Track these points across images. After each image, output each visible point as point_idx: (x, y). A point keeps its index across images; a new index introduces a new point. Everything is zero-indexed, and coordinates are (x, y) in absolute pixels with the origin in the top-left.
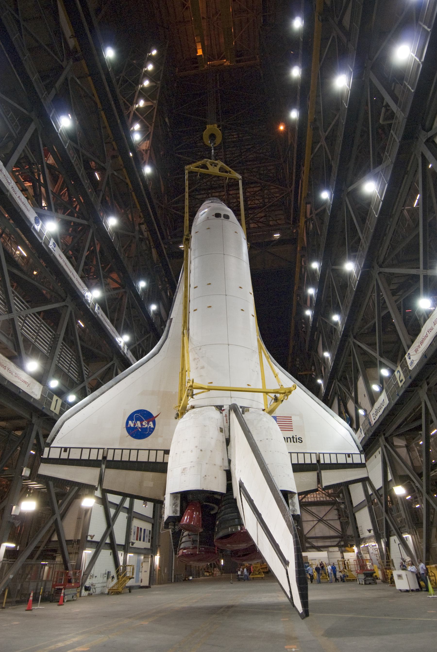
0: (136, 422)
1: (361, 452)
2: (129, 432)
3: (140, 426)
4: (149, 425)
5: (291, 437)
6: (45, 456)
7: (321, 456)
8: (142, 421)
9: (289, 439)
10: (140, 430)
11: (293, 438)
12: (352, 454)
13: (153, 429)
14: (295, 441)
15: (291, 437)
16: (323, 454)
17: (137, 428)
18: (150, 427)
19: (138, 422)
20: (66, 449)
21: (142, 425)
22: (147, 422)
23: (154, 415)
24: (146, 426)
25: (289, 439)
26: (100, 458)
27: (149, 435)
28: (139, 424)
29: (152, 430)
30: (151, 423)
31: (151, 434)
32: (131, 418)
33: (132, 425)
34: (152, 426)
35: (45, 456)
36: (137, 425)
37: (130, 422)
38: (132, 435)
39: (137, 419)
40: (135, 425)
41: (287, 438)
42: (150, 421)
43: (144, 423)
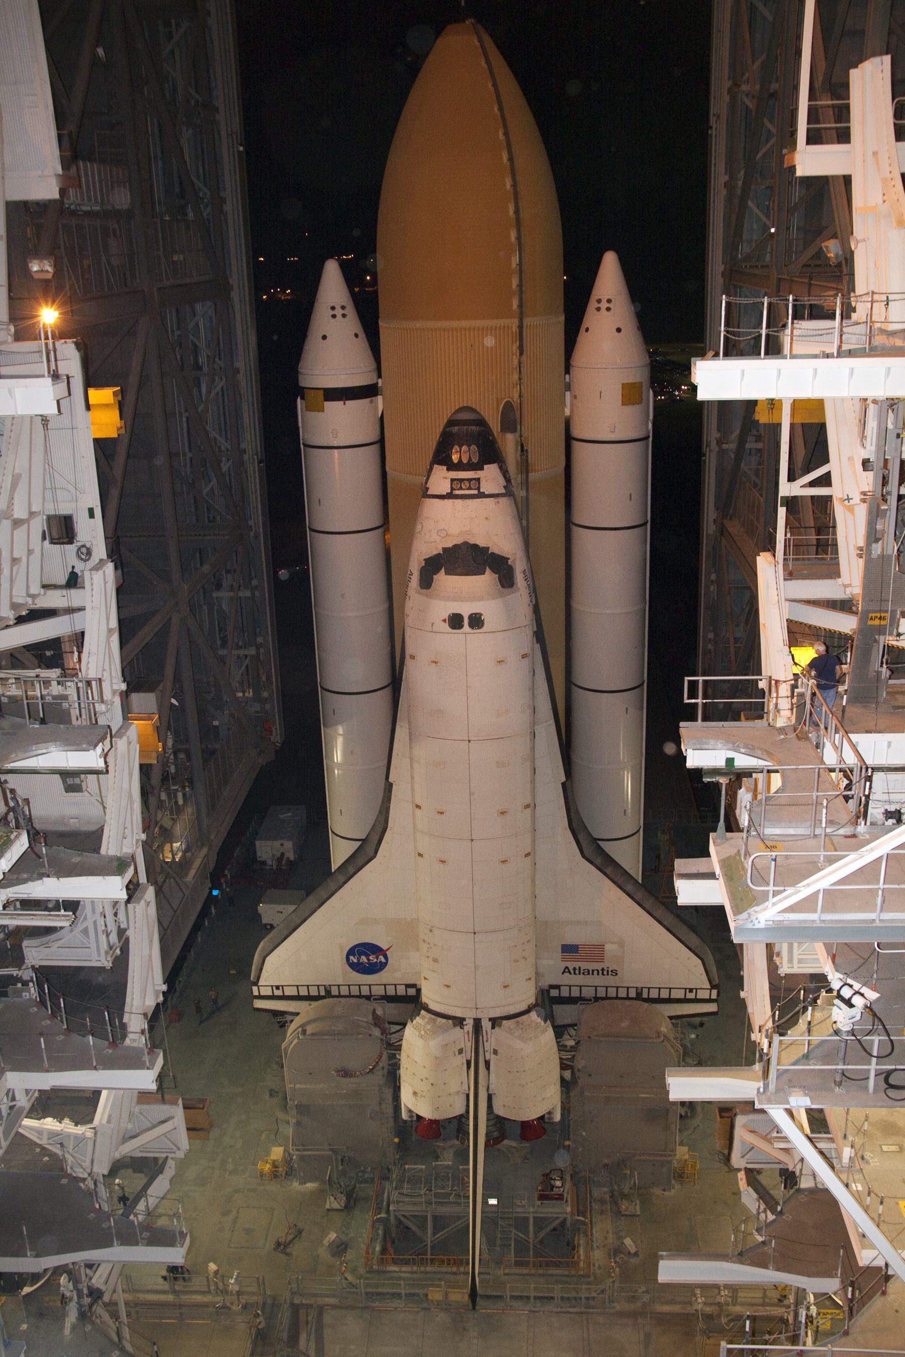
1: (713, 987)
2: (353, 969)
3: (366, 961)
5: (600, 969)
6: (256, 993)
7: (645, 991)
8: (367, 956)
9: (595, 972)
11: (603, 970)
12: (696, 989)
14: (605, 973)
15: (600, 969)
16: (649, 988)
17: (362, 963)
20: (278, 988)
21: (368, 960)
25: (595, 972)
26: (323, 993)
27: (380, 970)
28: (364, 959)
29: (383, 966)
32: (351, 952)
33: (355, 961)
34: (383, 960)
35: (256, 993)
38: (358, 971)
39: (360, 954)
41: (593, 971)
43: (371, 958)
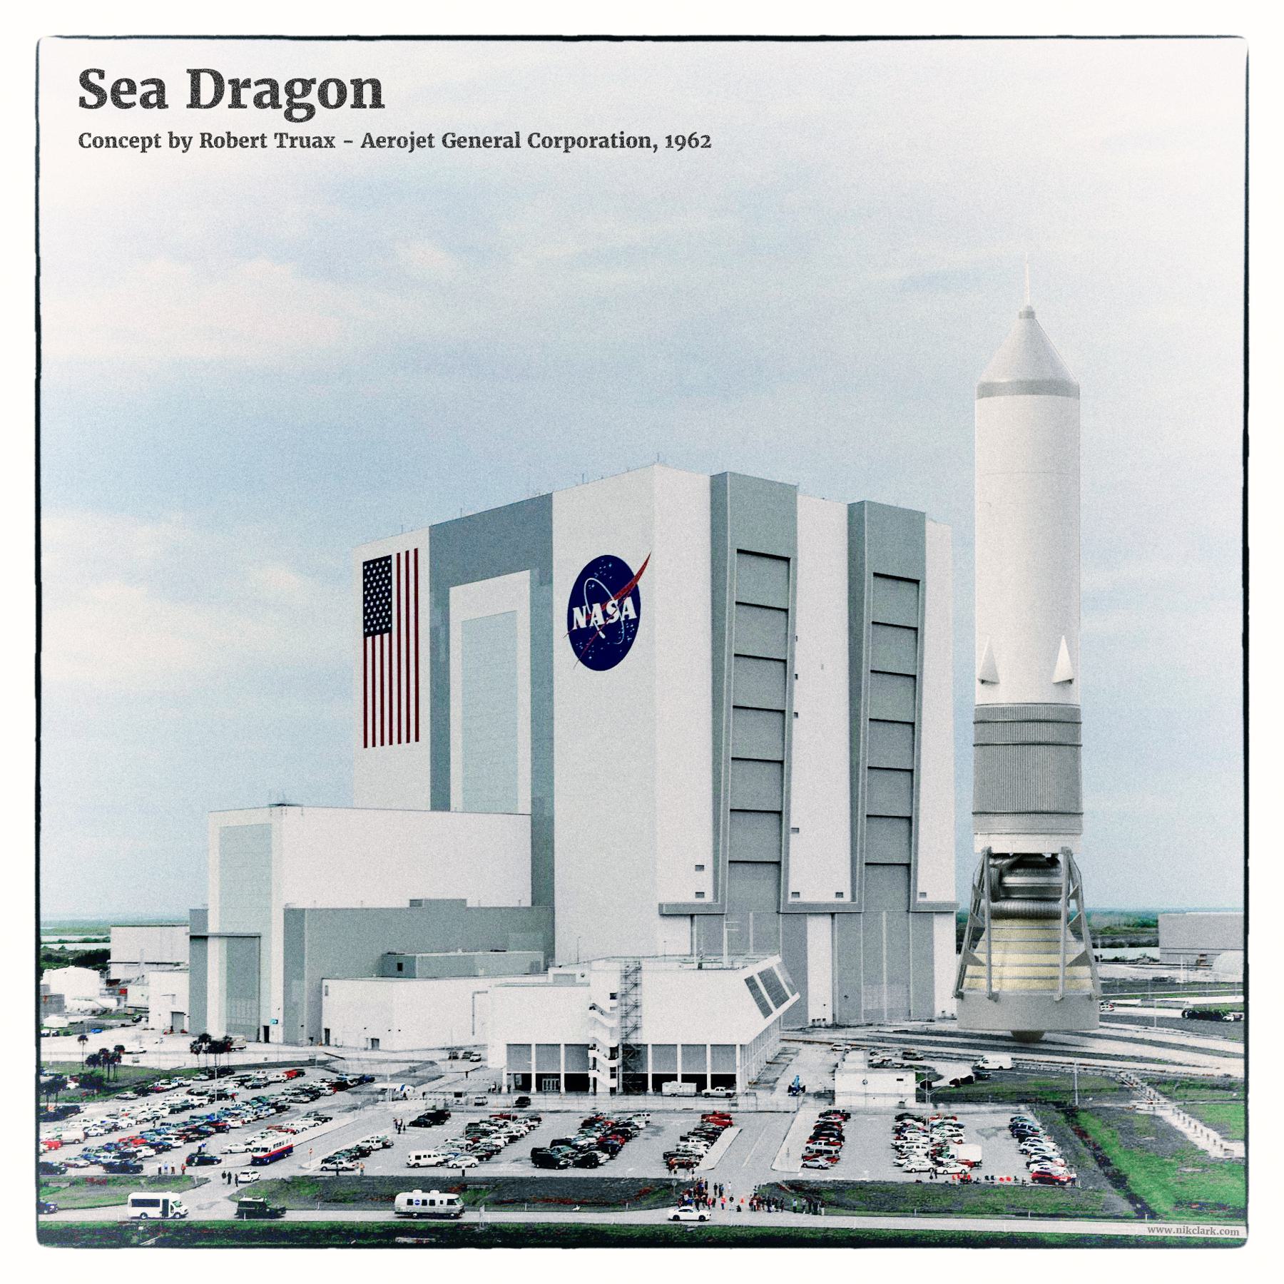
0: (591, 608)
3: (601, 622)
4: (624, 613)
8: (603, 600)
10: (603, 636)
18: (627, 616)
19: (597, 607)
21: (605, 615)
22: (616, 602)
23: (635, 573)
27: (627, 647)
30: (628, 602)
31: (632, 642)
33: (583, 625)
34: (633, 616)
36: (593, 620)
37: (576, 610)
40: (588, 622)
42: (625, 596)
43: (610, 610)
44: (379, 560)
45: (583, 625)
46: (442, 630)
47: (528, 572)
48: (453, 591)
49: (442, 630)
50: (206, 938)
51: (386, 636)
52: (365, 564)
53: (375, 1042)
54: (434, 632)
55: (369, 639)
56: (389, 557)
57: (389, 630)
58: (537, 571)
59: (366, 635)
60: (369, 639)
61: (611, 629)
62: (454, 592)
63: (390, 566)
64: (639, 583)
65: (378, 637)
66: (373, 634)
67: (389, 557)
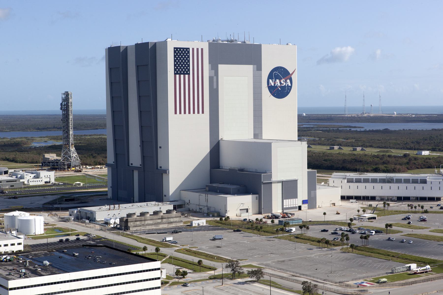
3: (279, 85)
8: (280, 79)
13: (291, 87)
18: (288, 85)
19: (278, 81)
21: (281, 83)
23: (291, 73)
24: (284, 84)
30: (288, 81)
32: (270, 76)
33: (273, 84)
34: (290, 85)
37: (270, 80)
38: (273, 95)
39: (277, 77)
40: (275, 84)
42: (287, 79)
43: (282, 82)
44: (183, 49)
45: (273, 84)
46: (215, 78)
47: (252, 66)
48: (220, 66)
49: (215, 78)
50: (271, 183)
51: (187, 76)
52: (174, 48)
53: (334, 204)
54: (211, 79)
55: (178, 76)
56: (189, 49)
57: (189, 74)
58: (256, 66)
59: (175, 74)
60: (178, 76)
61: (283, 88)
62: (220, 66)
63: (189, 52)
64: (292, 76)
65: (182, 76)
66: (180, 74)
67: (189, 49)
